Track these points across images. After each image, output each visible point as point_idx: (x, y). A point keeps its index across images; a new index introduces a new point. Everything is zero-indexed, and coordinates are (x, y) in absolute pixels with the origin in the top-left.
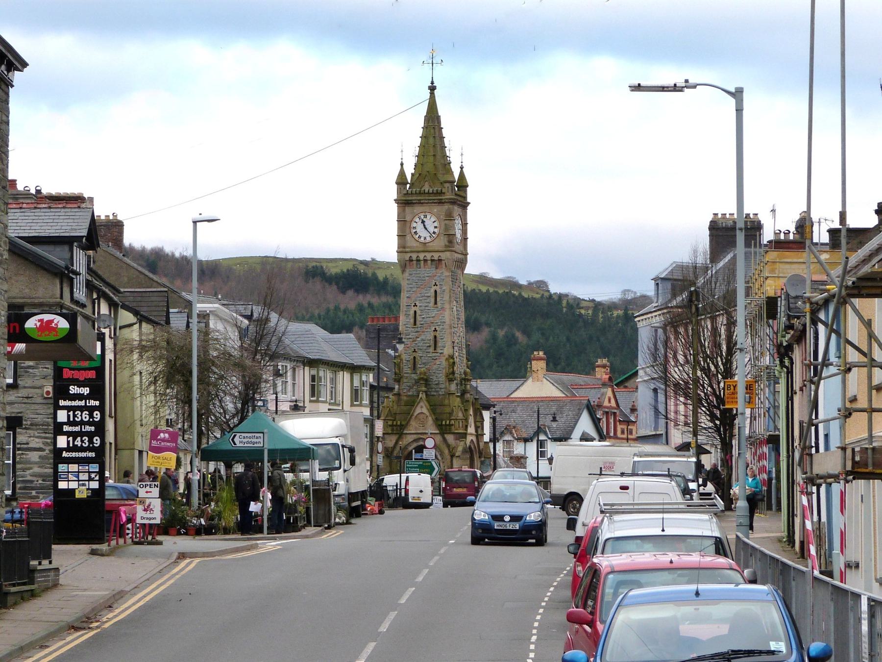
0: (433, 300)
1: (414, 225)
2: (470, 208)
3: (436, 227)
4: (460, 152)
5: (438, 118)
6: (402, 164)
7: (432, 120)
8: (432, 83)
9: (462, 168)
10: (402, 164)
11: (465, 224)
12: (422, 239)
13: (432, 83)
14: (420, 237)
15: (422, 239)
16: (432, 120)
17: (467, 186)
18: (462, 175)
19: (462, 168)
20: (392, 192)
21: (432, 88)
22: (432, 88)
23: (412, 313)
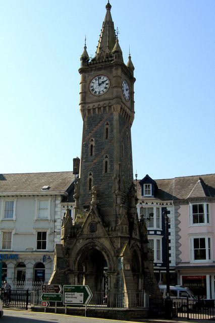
0: (105, 135)
1: (92, 84)
2: (136, 85)
3: (107, 84)
4: (130, 47)
5: (112, 24)
6: (85, 48)
7: (109, 25)
8: (109, 4)
9: (130, 58)
10: (85, 48)
11: (132, 93)
12: (97, 93)
13: (109, 4)
14: (96, 92)
15: (97, 93)
16: (109, 25)
17: (133, 69)
18: (130, 63)
19: (130, 58)
20: (79, 64)
21: (109, 7)
22: (109, 7)
23: (90, 145)
